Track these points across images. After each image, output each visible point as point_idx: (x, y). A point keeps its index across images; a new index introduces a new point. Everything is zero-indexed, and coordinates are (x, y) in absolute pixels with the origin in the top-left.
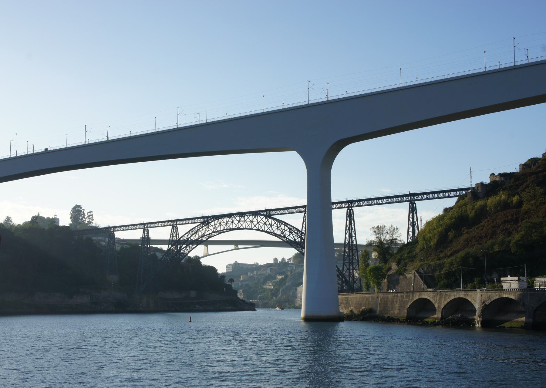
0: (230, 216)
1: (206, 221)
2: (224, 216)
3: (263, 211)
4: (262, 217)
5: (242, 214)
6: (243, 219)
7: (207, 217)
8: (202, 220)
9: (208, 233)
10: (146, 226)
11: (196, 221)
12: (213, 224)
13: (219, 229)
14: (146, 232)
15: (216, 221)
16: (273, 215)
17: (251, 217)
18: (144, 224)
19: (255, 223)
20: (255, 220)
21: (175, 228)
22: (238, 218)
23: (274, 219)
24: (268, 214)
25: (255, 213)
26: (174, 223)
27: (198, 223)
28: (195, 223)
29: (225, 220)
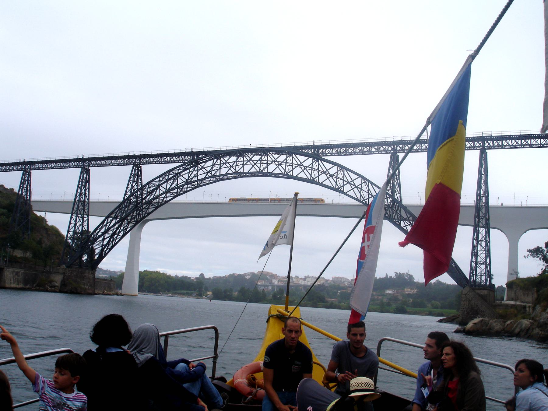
0: (240, 153)
1: (195, 159)
2: (229, 153)
3: (308, 147)
4: (302, 158)
5: (265, 151)
7: (198, 153)
9: (196, 179)
10: (27, 167)
12: (210, 163)
13: (218, 173)
14: (86, 172)
15: (215, 160)
17: (283, 157)
18: (83, 160)
21: (137, 168)
24: (316, 152)
25: (292, 151)
26: (137, 161)
28: (173, 162)
29: (234, 159)
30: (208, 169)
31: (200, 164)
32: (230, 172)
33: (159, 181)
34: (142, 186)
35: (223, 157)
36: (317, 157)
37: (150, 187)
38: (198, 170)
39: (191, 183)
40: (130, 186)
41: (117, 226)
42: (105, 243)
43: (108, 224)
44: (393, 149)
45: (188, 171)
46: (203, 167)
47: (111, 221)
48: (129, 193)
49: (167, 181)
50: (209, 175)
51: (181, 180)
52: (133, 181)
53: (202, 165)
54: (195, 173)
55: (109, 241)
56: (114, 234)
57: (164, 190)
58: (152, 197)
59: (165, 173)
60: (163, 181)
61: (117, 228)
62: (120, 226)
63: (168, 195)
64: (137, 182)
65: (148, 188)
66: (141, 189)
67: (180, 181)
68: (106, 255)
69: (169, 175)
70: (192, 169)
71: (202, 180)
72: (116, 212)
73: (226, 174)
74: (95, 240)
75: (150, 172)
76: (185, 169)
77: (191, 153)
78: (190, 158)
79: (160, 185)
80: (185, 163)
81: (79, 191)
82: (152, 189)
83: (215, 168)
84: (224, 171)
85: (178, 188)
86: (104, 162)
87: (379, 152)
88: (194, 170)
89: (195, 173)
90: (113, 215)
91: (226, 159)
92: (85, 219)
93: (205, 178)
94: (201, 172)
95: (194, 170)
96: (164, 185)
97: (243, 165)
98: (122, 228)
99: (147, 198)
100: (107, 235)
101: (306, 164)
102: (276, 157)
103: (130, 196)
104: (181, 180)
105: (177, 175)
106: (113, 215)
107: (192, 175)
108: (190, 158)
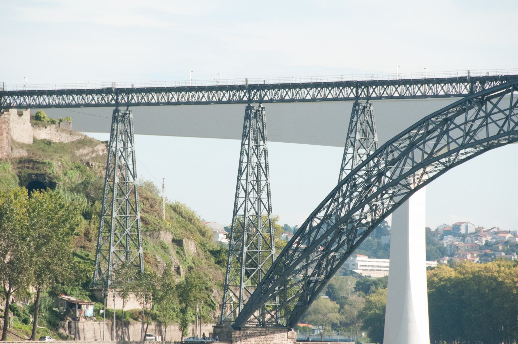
7: (483, 80)
8: (464, 89)
11: (447, 88)
31: (489, 99)
33: (409, 138)
37: (392, 152)
41: (332, 234)
42: (310, 271)
43: (314, 234)
48: (349, 166)
54: (478, 122)
58: (397, 173)
60: (417, 137)
61: (333, 240)
63: (428, 169)
65: (387, 154)
69: (428, 125)
70: (472, 113)
72: (329, 206)
76: (458, 114)
77: (473, 80)
81: (245, 159)
82: (396, 154)
88: (476, 118)
89: (478, 122)
90: (321, 215)
95: (476, 118)
98: (344, 238)
99: (388, 174)
103: (354, 172)
106: (321, 215)
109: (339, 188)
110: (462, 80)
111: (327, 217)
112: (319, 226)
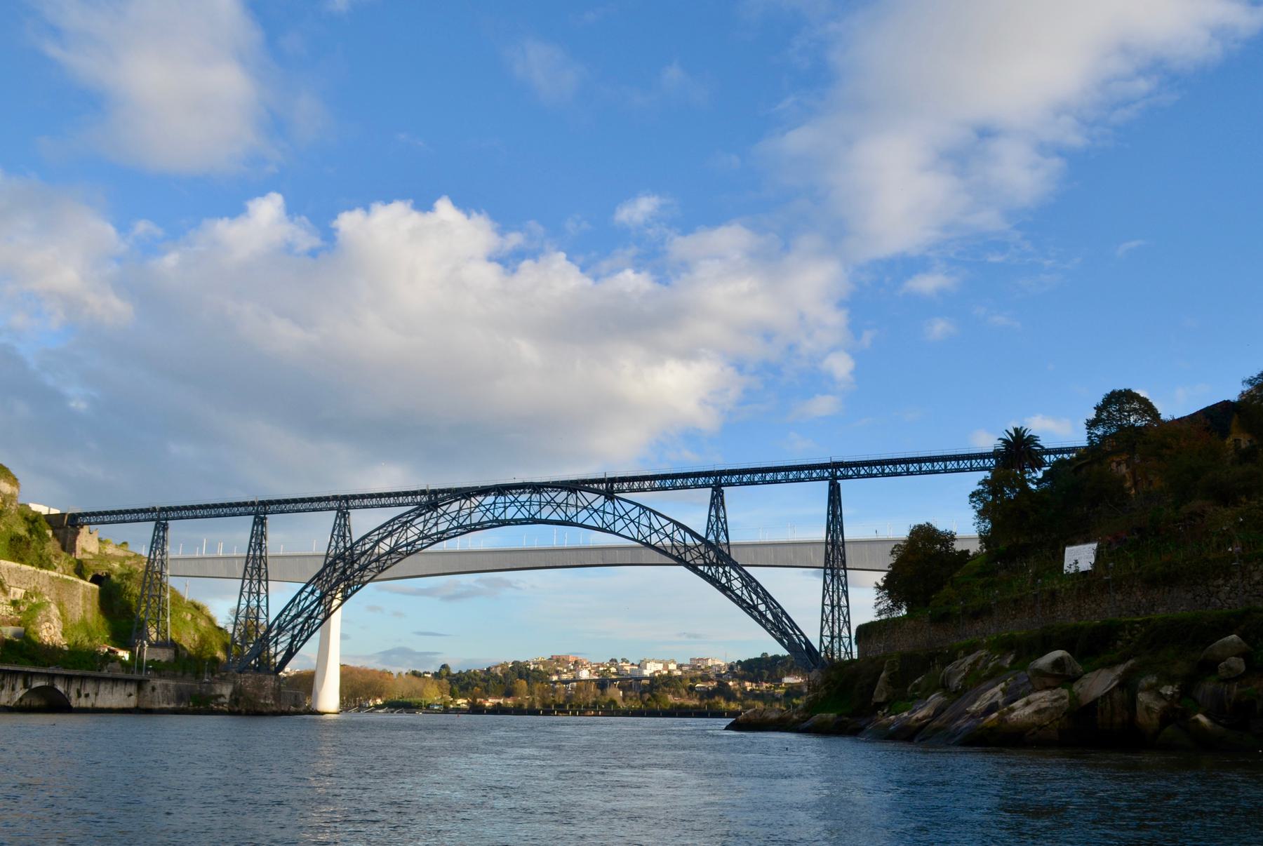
1: (432, 500)
2: (485, 491)
4: (591, 496)
5: (537, 488)
6: (536, 497)
7: (435, 492)
9: (434, 530)
12: (456, 506)
13: (468, 522)
16: (623, 491)
19: (571, 511)
20: (572, 500)
21: (343, 514)
22: (523, 498)
23: (618, 498)
24: (609, 488)
25: (573, 486)
26: (343, 504)
27: (408, 505)
29: (490, 499)
30: (453, 515)
32: (485, 519)
34: (353, 545)
35: (474, 496)
36: (610, 495)
38: (438, 517)
39: (426, 537)
40: (334, 543)
42: (296, 632)
44: (715, 482)
45: (422, 518)
46: (445, 513)
47: (306, 598)
49: (391, 534)
50: (455, 523)
51: (412, 534)
52: (338, 536)
53: (444, 508)
55: (302, 629)
56: (310, 617)
57: (387, 549)
59: (388, 523)
62: (319, 604)
64: (344, 536)
66: (351, 548)
67: (410, 533)
68: (297, 650)
71: (443, 533)
73: (479, 523)
74: (281, 629)
75: (363, 522)
78: (425, 499)
79: (381, 540)
80: (419, 504)
83: (462, 513)
84: (476, 517)
85: (407, 545)
86: (300, 506)
87: (697, 486)
89: (433, 521)
90: (309, 589)
91: (480, 498)
92: (262, 596)
93: (448, 530)
94: (442, 519)
96: (387, 541)
97: (505, 508)
99: (363, 559)
100: (300, 620)
101: (596, 505)
102: (553, 494)
104: (412, 534)
105: (406, 525)
106: (309, 589)
107: (429, 525)
108: (425, 499)
109: (323, 570)
110: (423, 492)
111: (312, 592)
112: (306, 598)
